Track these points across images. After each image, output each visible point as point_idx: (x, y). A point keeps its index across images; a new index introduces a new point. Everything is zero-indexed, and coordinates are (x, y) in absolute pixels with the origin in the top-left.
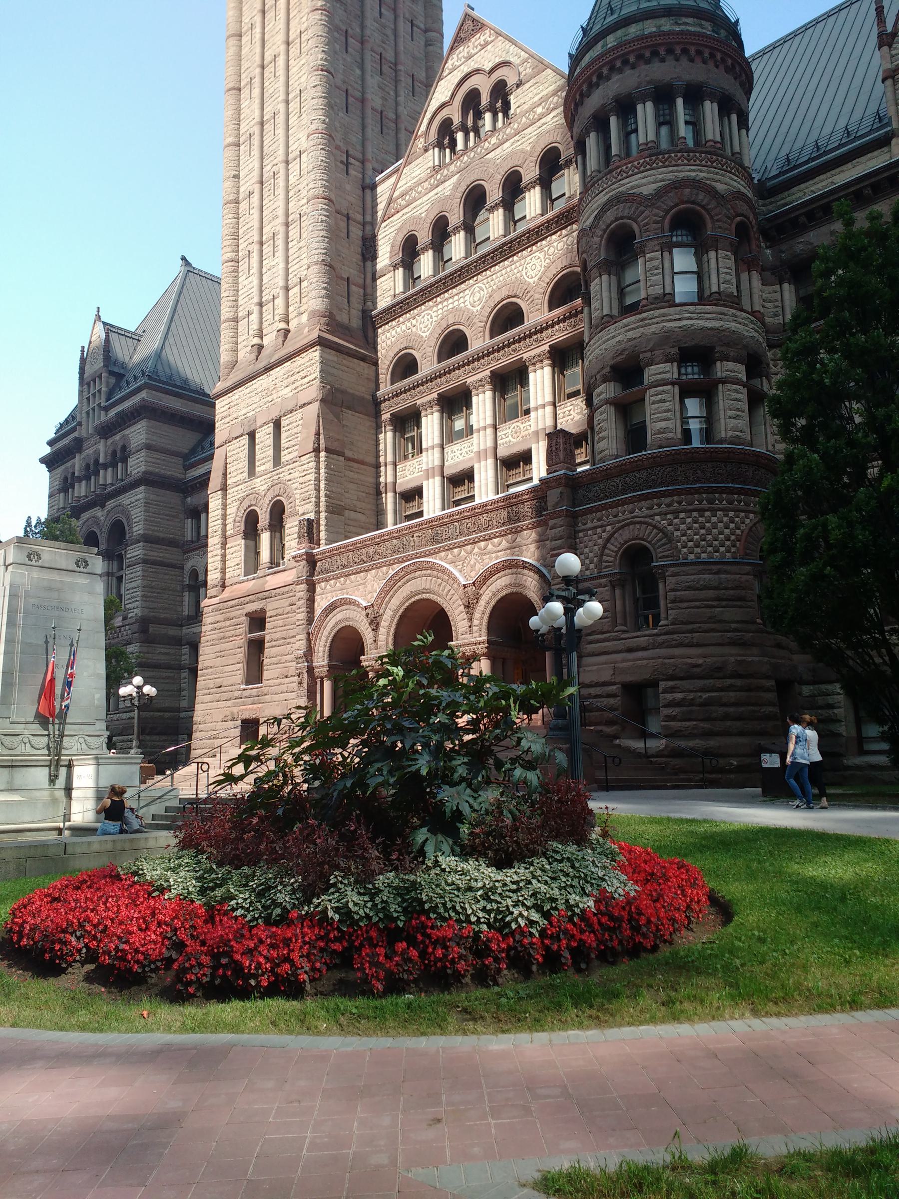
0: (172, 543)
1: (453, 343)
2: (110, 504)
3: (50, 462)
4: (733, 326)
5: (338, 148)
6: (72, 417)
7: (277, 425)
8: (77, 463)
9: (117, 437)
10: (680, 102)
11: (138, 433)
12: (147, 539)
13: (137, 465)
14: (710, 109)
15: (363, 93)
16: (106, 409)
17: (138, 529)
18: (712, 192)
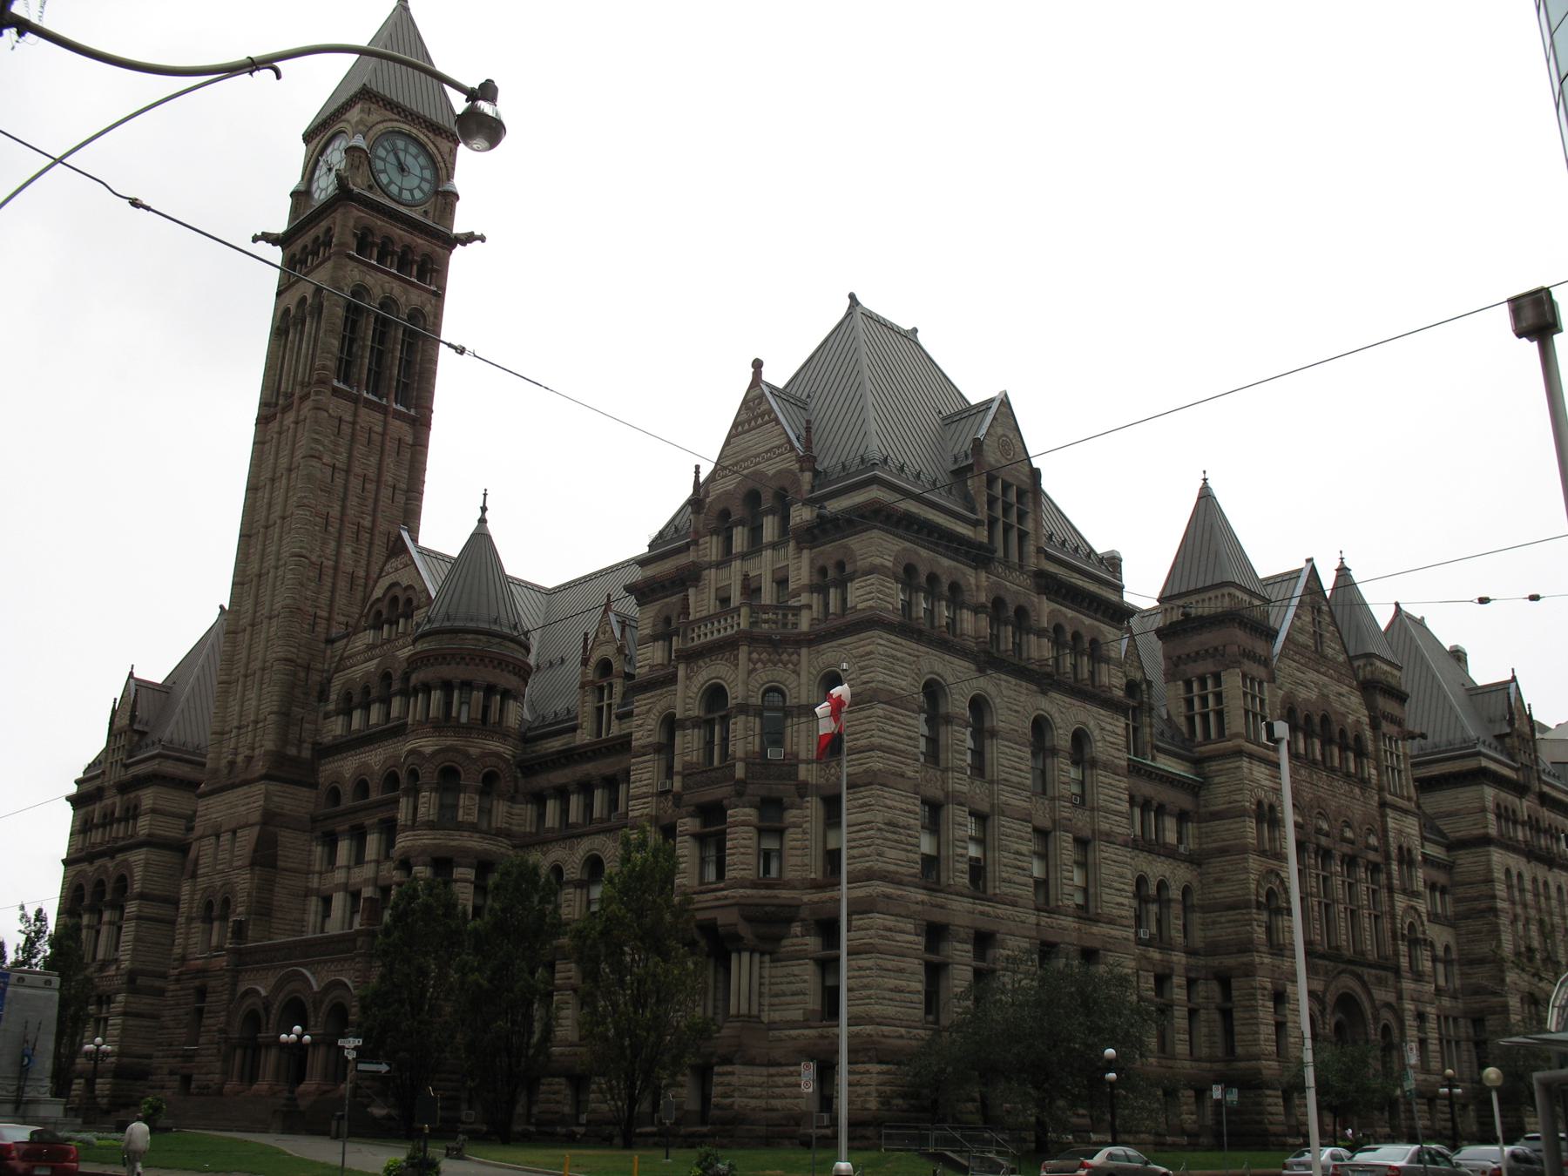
0: (165, 900)
1: (362, 787)
2: (120, 857)
3: (74, 801)
7: (234, 832)
8: (97, 809)
9: (132, 795)
10: (456, 694)
11: (147, 798)
12: (142, 896)
13: (143, 826)
14: (478, 696)
15: (337, 562)
16: (126, 766)
17: (137, 887)
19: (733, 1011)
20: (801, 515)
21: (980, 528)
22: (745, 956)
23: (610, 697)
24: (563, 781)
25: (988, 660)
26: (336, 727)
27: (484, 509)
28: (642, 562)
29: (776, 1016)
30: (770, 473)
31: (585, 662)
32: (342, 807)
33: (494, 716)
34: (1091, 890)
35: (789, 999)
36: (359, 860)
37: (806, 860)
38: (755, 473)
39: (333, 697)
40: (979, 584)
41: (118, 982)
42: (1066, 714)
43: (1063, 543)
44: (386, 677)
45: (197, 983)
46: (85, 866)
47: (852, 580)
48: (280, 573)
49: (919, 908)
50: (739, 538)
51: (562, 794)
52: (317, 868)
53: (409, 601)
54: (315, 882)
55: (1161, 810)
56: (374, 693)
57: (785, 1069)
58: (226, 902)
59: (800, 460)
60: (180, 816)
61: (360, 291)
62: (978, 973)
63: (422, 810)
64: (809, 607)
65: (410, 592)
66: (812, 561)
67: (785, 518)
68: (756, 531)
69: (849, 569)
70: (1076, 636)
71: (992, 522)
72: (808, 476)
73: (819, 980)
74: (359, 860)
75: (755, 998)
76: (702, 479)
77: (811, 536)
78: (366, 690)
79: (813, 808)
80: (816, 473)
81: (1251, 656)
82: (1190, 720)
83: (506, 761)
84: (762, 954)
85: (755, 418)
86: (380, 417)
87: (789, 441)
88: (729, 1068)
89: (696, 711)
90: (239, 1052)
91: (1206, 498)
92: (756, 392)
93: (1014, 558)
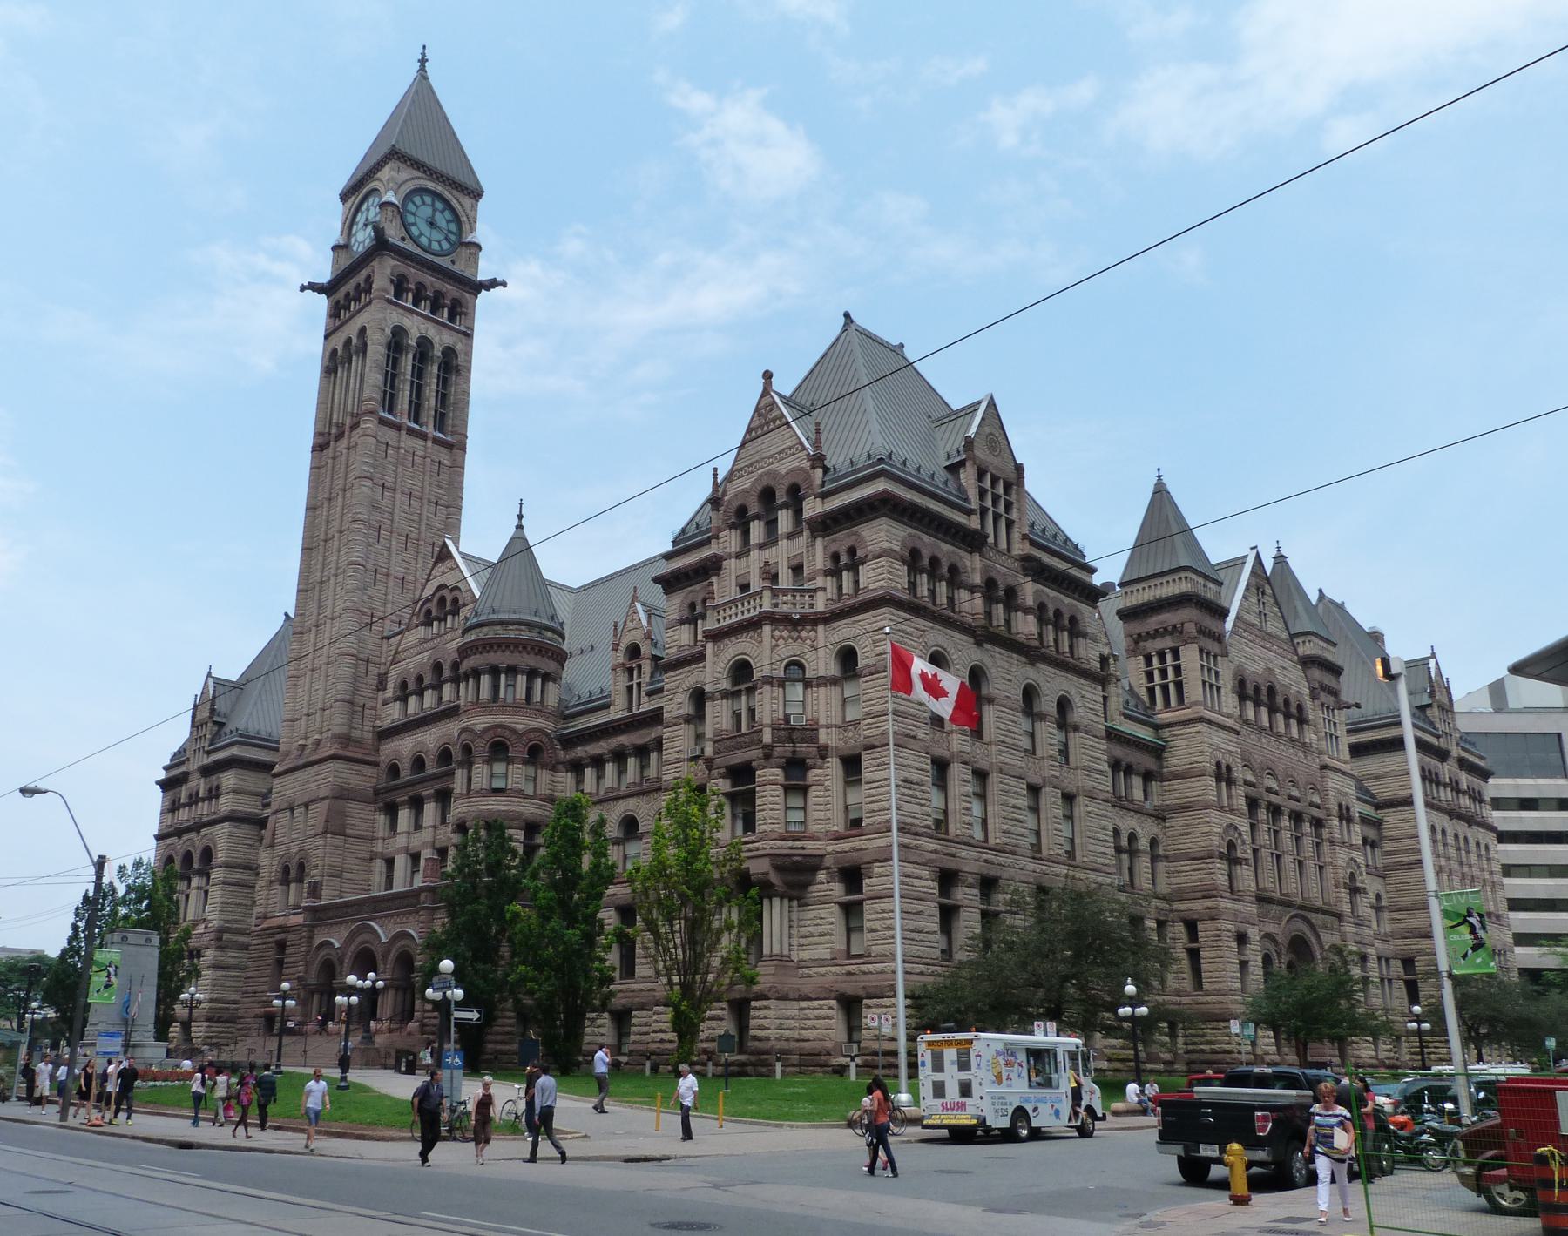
0: (247, 867)
1: (419, 763)
2: (204, 831)
3: (165, 785)
4: (518, 808)
5: (363, 613)
6: (182, 751)
7: (306, 805)
10: (503, 677)
11: (228, 779)
12: (229, 866)
14: (521, 680)
16: (208, 753)
18: (514, 731)
19: (766, 951)
20: (813, 508)
21: (973, 517)
22: (776, 901)
23: (639, 676)
24: (598, 751)
25: (983, 636)
26: (393, 714)
27: (520, 517)
28: (668, 557)
29: (805, 955)
30: (783, 472)
31: (616, 647)
32: (401, 781)
33: (537, 697)
34: (1077, 841)
35: (816, 940)
36: (418, 826)
37: (829, 814)
38: (769, 473)
39: (390, 686)
40: (974, 567)
41: (206, 939)
42: (1052, 684)
43: (1044, 530)
44: (437, 667)
45: (278, 937)
46: (174, 840)
47: (863, 563)
48: (340, 579)
49: (933, 856)
50: (757, 530)
51: (598, 762)
52: (381, 834)
53: (455, 600)
54: (379, 847)
55: (1129, 770)
56: (427, 681)
57: (815, 1003)
58: (301, 867)
59: (810, 458)
60: (257, 795)
61: (399, 332)
62: (985, 914)
63: (475, 779)
64: (824, 589)
65: (456, 593)
66: (825, 548)
67: (798, 512)
68: (772, 524)
69: (860, 554)
70: (1058, 613)
71: (984, 511)
72: (819, 471)
73: (843, 922)
74: (418, 826)
75: (786, 939)
76: (720, 478)
77: (826, 525)
78: (420, 679)
79: (834, 767)
80: (826, 470)
81: (1202, 631)
82: (1151, 691)
83: (548, 735)
84: (791, 900)
85: (768, 424)
86: (420, 442)
87: (801, 443)
88: (765, 1003)
89: (725, 685)
90: (316, 998)
91: (1161, 493)
92: (766, 400)
93: (1003, 545)
